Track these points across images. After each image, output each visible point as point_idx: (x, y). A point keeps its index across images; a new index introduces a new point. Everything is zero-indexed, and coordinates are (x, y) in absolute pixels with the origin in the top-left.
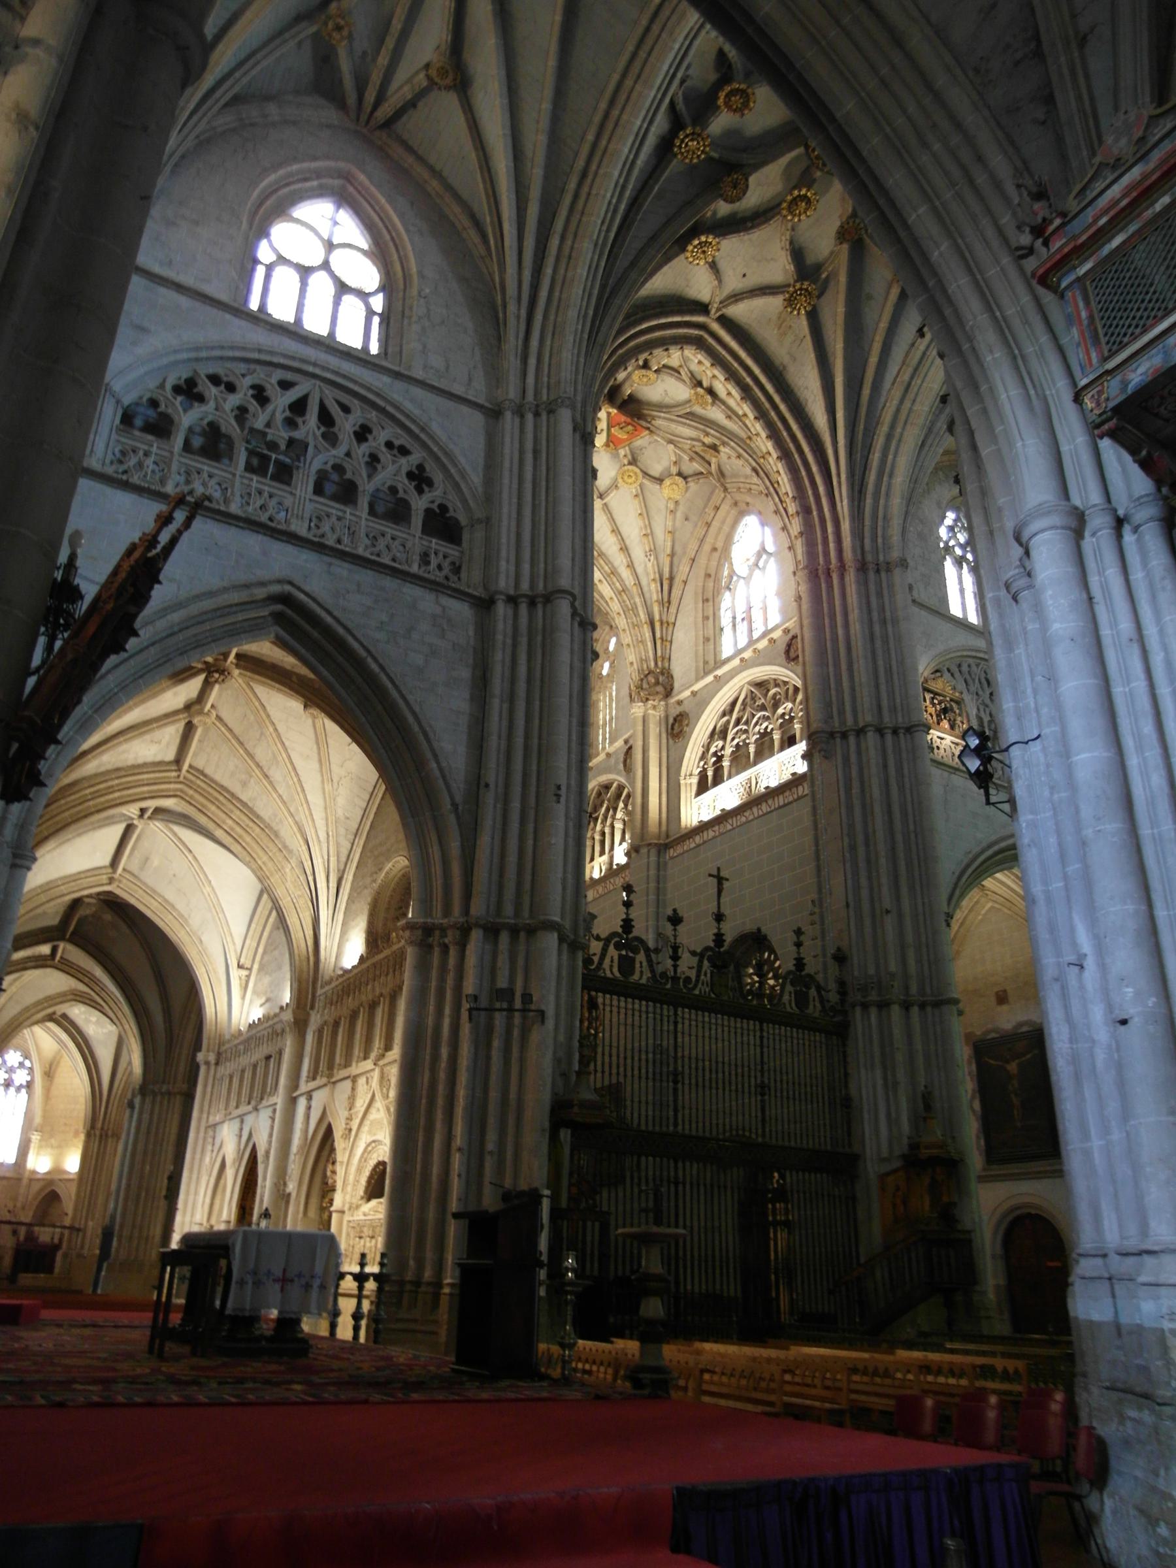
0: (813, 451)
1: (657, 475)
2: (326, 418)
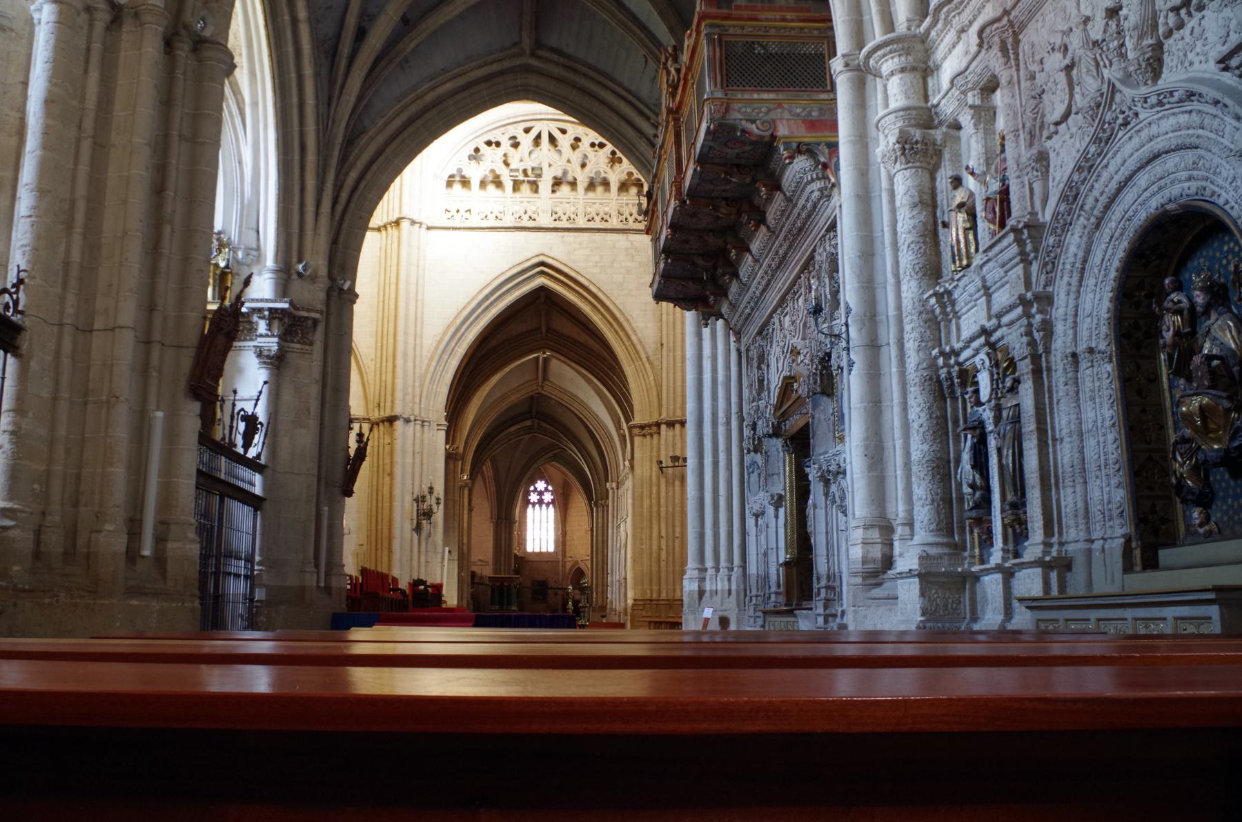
2: (552, 140)
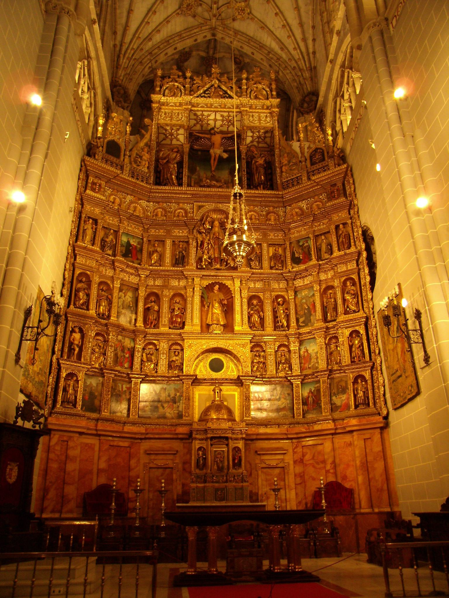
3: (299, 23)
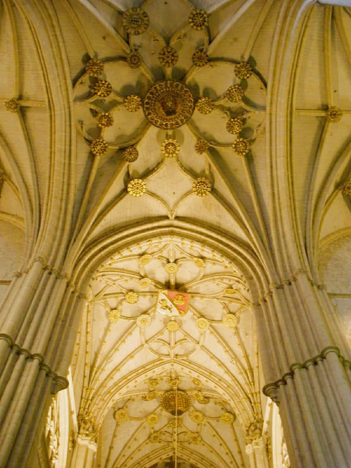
0: (247, 251)
1: (220, 319)
3: (239, 452)
